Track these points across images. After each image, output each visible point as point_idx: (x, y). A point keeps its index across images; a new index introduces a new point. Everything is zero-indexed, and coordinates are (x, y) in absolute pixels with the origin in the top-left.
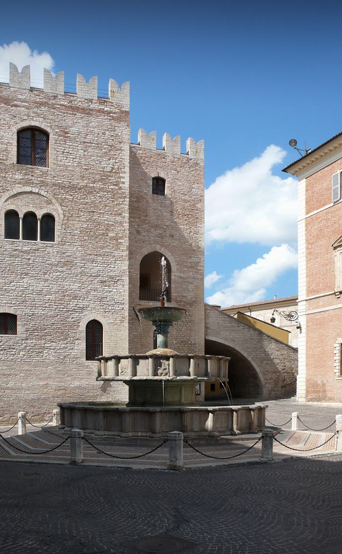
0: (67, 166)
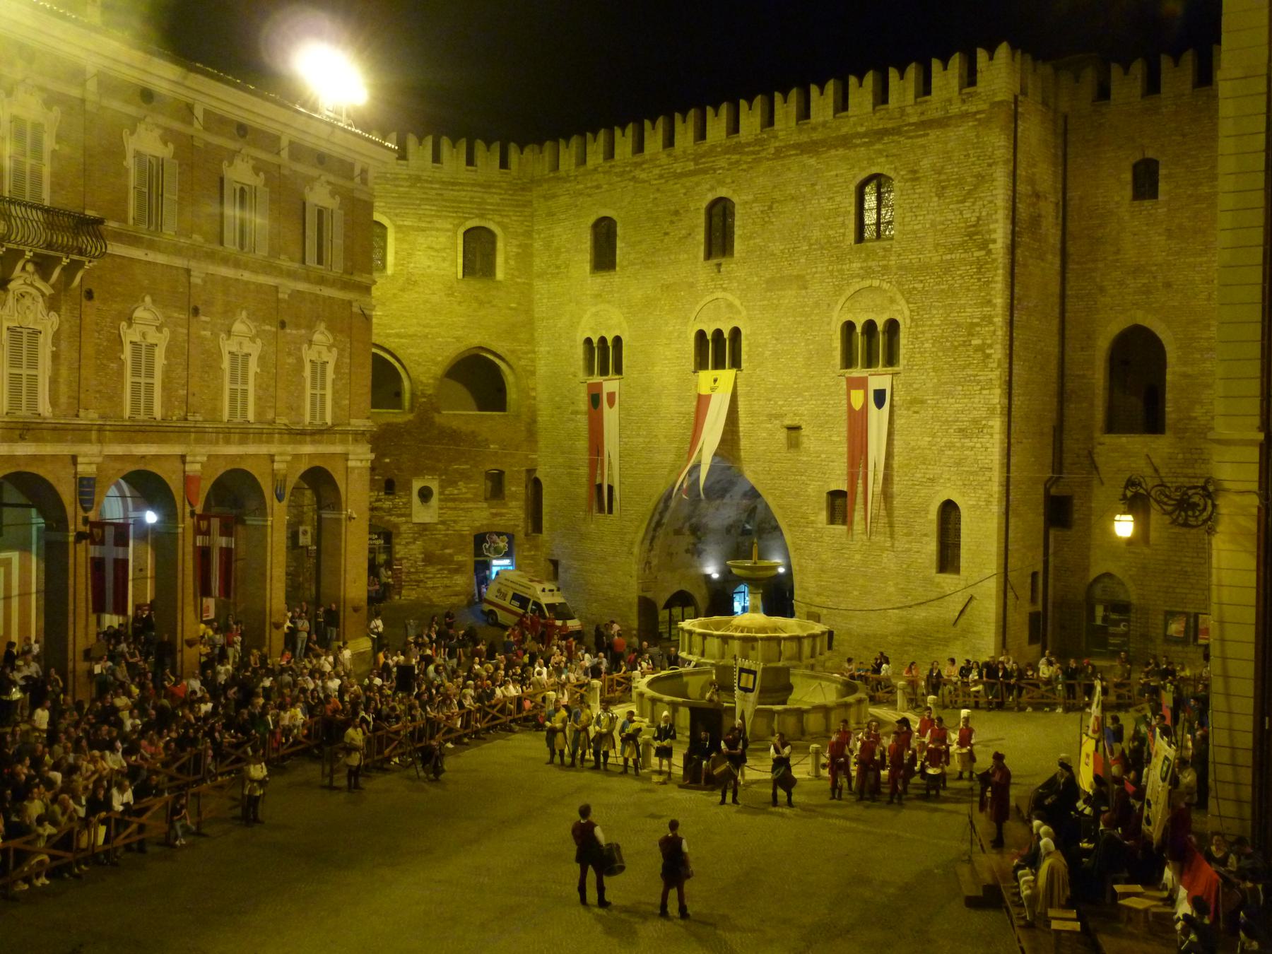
0: (914, 232)
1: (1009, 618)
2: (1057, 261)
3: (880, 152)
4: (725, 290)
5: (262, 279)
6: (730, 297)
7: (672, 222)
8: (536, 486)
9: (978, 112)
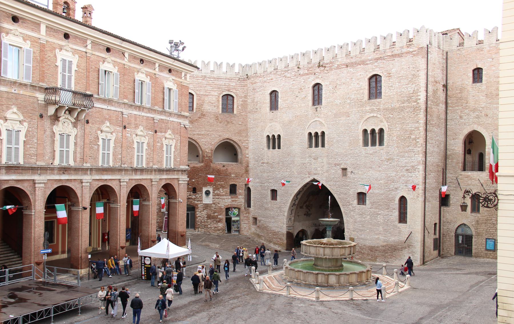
0: (390, 96)
1: (426, 240)
2: (444, 106)
3: (376, 66)
4: (319, 117)
5: (149, 115)
6: (321, 120)
7: (299, 92)
8: (249, 190)
9: (412, 52)
